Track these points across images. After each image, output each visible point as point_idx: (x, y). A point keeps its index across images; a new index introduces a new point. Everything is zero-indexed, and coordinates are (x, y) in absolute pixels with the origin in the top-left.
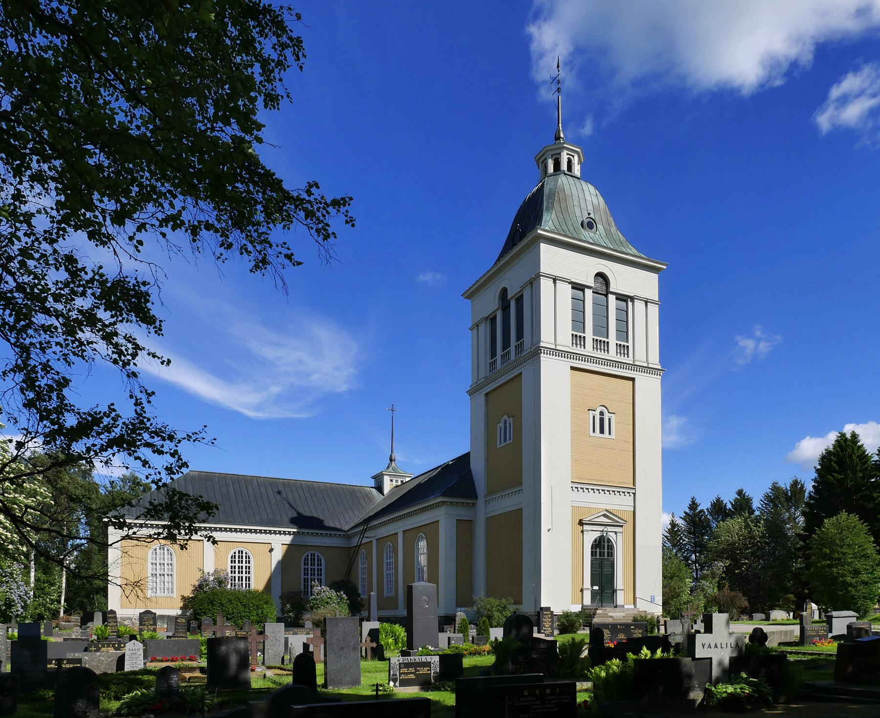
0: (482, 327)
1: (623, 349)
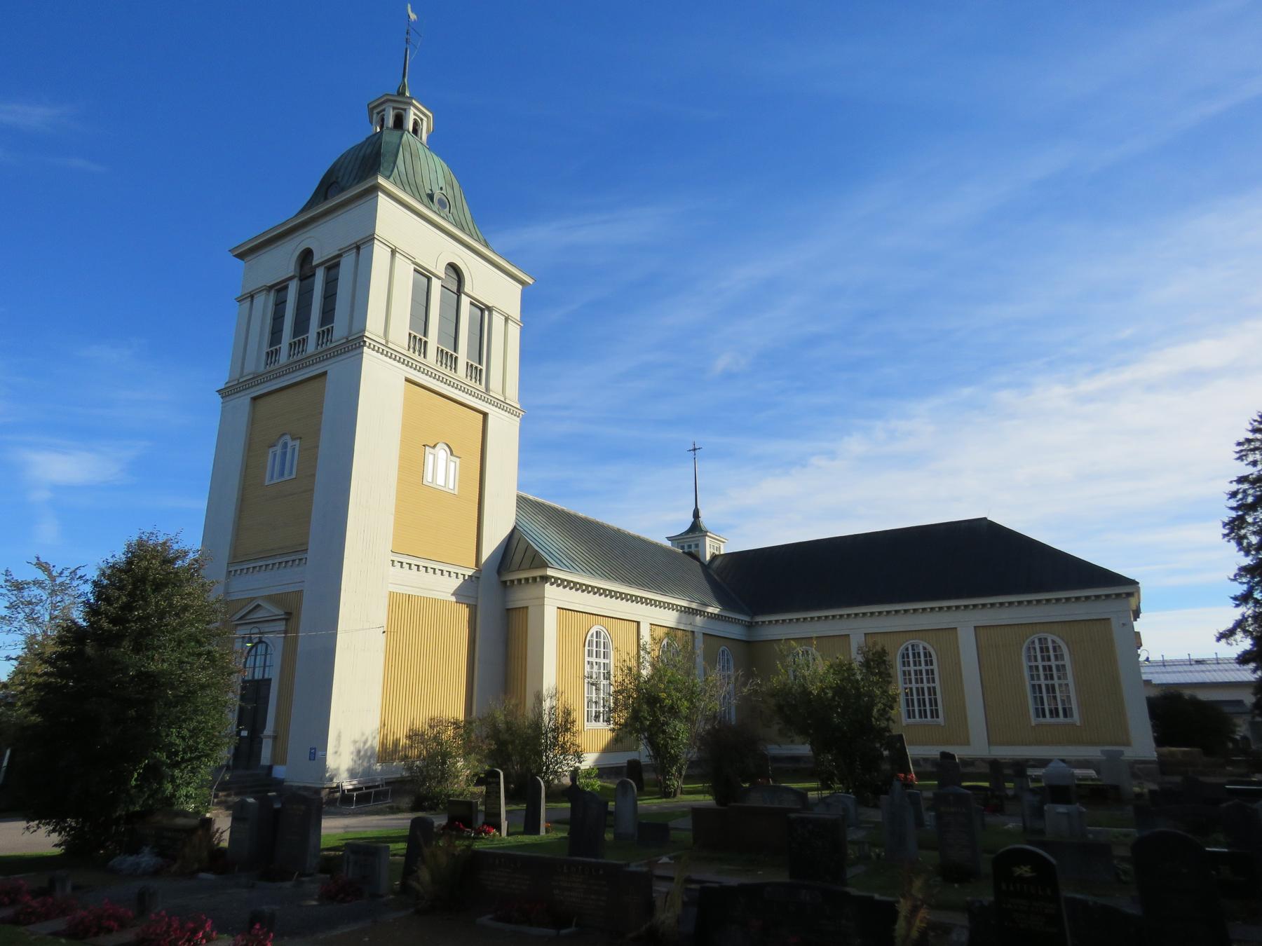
0: (260, 300)
1: (475, 372)
